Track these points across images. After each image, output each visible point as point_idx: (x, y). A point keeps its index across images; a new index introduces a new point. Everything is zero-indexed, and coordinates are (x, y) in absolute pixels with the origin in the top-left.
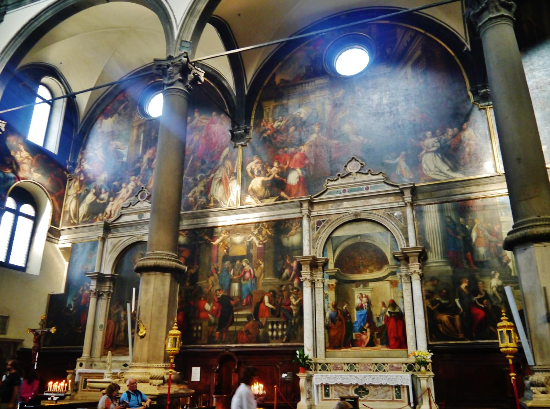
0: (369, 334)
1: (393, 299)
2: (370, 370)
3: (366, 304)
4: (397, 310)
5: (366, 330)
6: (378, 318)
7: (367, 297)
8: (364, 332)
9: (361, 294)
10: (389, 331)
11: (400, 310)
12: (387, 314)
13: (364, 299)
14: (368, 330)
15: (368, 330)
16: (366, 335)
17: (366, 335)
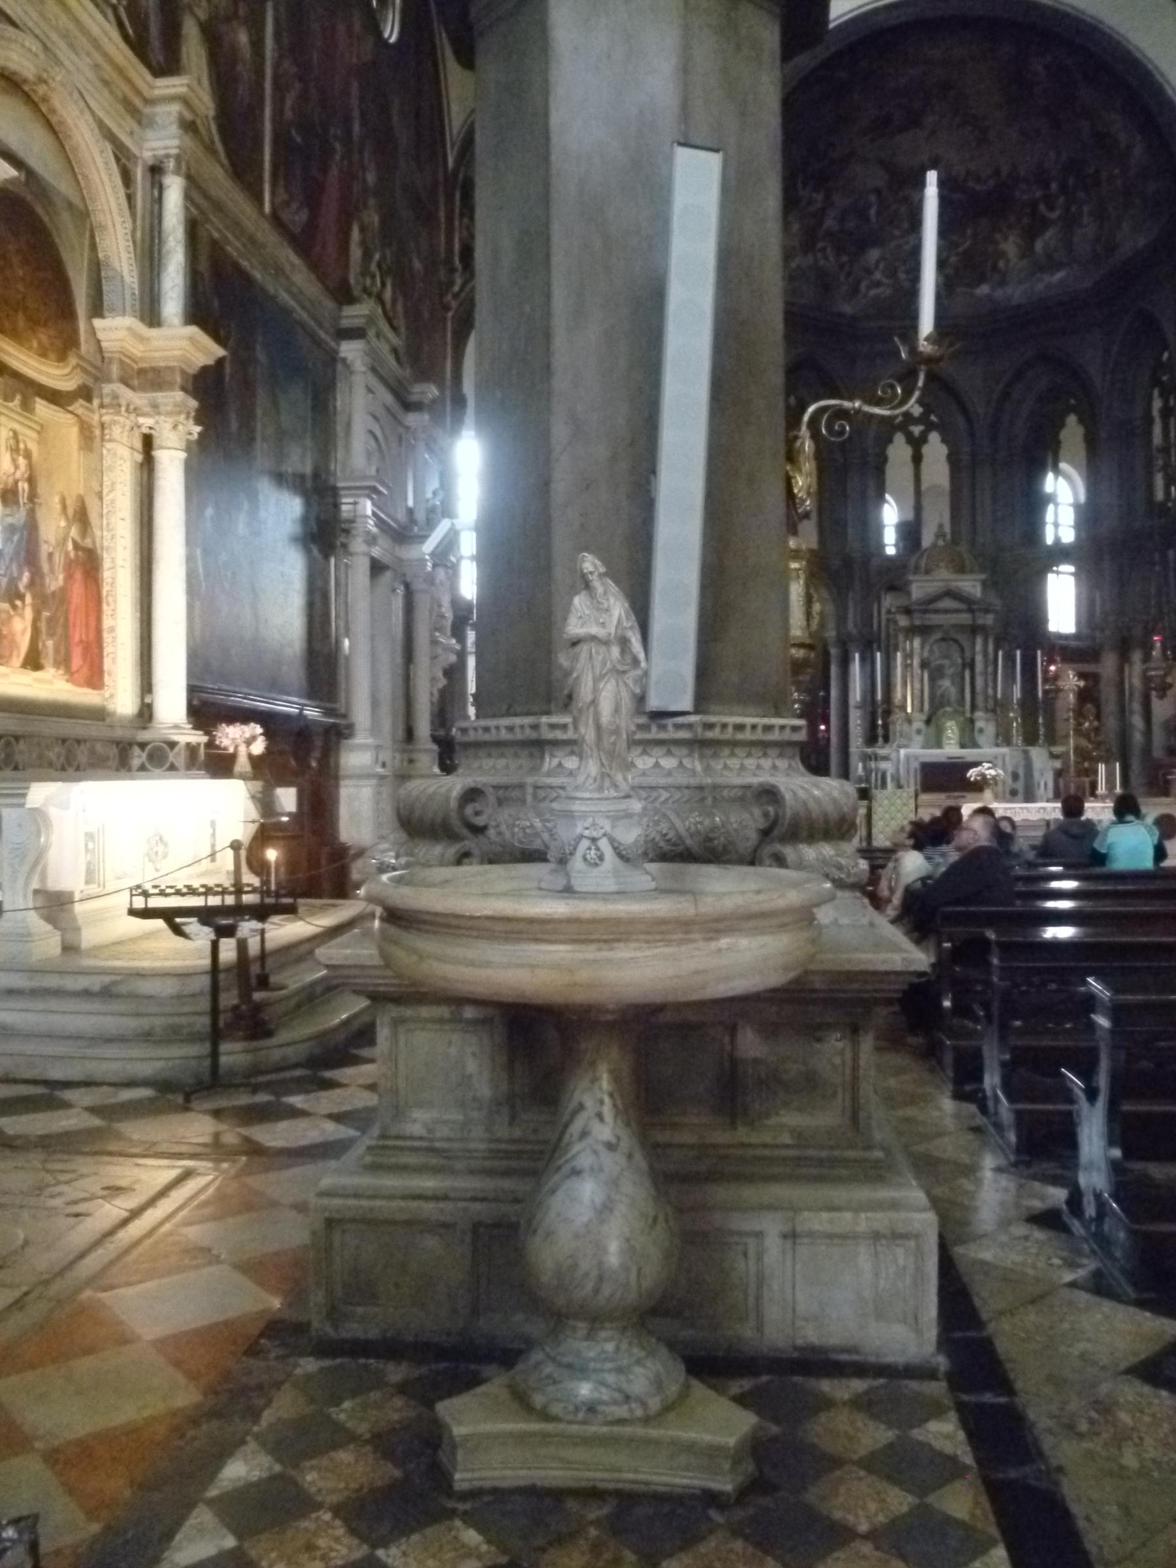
0: (29, 613)
1: (82, 493)
2: (51, 765)
3: (26, 486)
4: (88, 543)
5: (21, 597)
6: (50, 555)
7: (28, 455)
8: (18, 603)
9: (15, 433)
10: (71, 616)
11: (94, 542)
12: (70, 546)
13: (22, 461)
14: (28, 599)
15: (28, 599)
16: (22, 616)
17: (22, 616)
